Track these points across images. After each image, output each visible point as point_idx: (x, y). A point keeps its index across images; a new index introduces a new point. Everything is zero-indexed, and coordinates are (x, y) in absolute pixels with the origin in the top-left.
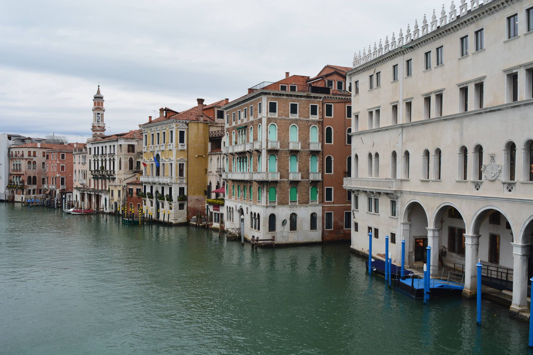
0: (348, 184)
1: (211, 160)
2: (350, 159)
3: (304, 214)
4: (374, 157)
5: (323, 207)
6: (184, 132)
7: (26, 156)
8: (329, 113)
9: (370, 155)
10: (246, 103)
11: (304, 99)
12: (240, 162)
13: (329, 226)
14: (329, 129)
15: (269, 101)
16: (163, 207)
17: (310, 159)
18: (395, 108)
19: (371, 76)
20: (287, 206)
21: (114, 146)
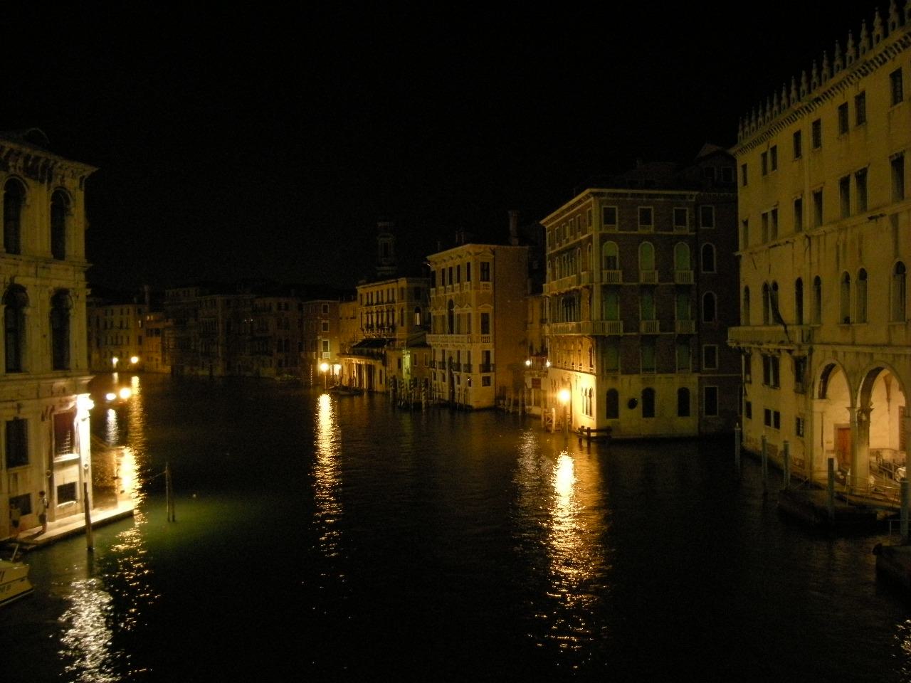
0: (736, 335)
1: (533, 307)
3: (666, 388)
4: (771, 291)
5: (700, 378)
6: (488, 263)
7: (274, 309)
8: (707, 222)
9: (766, 287)
11: (662, 200)
13: (711, 409)
14: (708, 250)
15: (603, 207)
16: (459, 383)
17: (675, 299)
18: (798, 204)
20: (636, 376)
21: (393, 289)
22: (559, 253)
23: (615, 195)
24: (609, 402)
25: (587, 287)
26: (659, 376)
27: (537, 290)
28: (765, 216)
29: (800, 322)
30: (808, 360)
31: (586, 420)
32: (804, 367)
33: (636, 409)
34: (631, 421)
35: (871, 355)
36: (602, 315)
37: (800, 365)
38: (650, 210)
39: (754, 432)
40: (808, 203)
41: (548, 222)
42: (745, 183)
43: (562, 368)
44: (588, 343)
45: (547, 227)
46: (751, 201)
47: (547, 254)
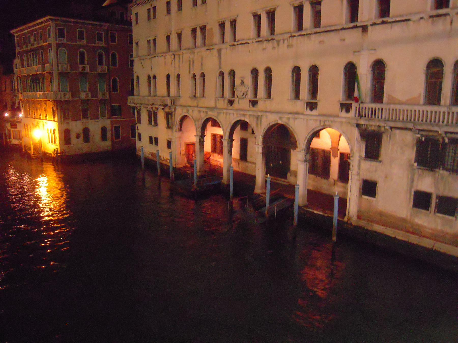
2: (132, 80)
3: (95, 127)
4: (151, 79)
5: (111, 121)
8: (113, 40)
9: (149, 77)
10: (35, 28)
11: (91, 26)
12: (33, 83)
13: (117, 136)
14: (114, 55)
15: (57, 27)
18: (168, 38)
19: (149, 10)
22: (27, 52)
23: (64, 21)
24: (66, 136)
25: (50, 73)
26: (91, 121)
27: (9, 71)
28: (149, 41)
29: (169, 95)
30: (173, 113)
31: (52, 147)
32: (171, 117)
33: (79, 140)
34: (78, 145)
35: (207, 112)
36: (59, 89)
37: (168, 115)
38: (83, 31)
39: (144, 148)
40: (174, 38)
41: (16, 32)
42: (137, 23)
43: (32, 118)
44: (50, 105)
45: (15, 35)
46: (140, 33)
47: (17, 51)
